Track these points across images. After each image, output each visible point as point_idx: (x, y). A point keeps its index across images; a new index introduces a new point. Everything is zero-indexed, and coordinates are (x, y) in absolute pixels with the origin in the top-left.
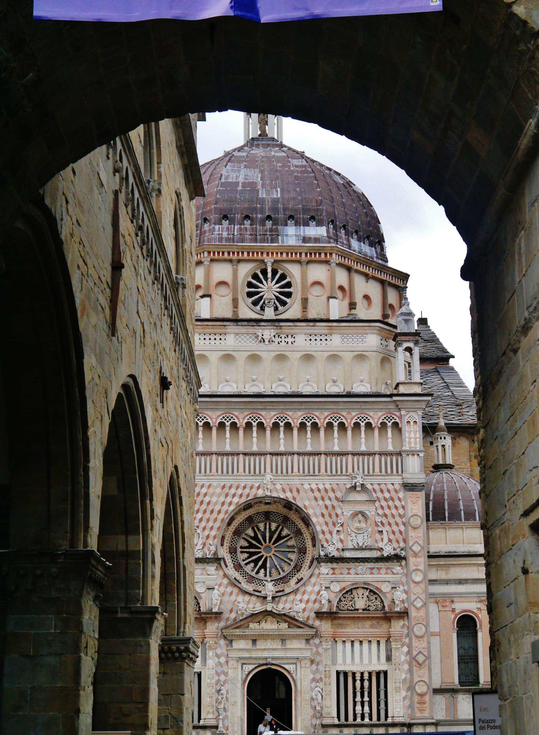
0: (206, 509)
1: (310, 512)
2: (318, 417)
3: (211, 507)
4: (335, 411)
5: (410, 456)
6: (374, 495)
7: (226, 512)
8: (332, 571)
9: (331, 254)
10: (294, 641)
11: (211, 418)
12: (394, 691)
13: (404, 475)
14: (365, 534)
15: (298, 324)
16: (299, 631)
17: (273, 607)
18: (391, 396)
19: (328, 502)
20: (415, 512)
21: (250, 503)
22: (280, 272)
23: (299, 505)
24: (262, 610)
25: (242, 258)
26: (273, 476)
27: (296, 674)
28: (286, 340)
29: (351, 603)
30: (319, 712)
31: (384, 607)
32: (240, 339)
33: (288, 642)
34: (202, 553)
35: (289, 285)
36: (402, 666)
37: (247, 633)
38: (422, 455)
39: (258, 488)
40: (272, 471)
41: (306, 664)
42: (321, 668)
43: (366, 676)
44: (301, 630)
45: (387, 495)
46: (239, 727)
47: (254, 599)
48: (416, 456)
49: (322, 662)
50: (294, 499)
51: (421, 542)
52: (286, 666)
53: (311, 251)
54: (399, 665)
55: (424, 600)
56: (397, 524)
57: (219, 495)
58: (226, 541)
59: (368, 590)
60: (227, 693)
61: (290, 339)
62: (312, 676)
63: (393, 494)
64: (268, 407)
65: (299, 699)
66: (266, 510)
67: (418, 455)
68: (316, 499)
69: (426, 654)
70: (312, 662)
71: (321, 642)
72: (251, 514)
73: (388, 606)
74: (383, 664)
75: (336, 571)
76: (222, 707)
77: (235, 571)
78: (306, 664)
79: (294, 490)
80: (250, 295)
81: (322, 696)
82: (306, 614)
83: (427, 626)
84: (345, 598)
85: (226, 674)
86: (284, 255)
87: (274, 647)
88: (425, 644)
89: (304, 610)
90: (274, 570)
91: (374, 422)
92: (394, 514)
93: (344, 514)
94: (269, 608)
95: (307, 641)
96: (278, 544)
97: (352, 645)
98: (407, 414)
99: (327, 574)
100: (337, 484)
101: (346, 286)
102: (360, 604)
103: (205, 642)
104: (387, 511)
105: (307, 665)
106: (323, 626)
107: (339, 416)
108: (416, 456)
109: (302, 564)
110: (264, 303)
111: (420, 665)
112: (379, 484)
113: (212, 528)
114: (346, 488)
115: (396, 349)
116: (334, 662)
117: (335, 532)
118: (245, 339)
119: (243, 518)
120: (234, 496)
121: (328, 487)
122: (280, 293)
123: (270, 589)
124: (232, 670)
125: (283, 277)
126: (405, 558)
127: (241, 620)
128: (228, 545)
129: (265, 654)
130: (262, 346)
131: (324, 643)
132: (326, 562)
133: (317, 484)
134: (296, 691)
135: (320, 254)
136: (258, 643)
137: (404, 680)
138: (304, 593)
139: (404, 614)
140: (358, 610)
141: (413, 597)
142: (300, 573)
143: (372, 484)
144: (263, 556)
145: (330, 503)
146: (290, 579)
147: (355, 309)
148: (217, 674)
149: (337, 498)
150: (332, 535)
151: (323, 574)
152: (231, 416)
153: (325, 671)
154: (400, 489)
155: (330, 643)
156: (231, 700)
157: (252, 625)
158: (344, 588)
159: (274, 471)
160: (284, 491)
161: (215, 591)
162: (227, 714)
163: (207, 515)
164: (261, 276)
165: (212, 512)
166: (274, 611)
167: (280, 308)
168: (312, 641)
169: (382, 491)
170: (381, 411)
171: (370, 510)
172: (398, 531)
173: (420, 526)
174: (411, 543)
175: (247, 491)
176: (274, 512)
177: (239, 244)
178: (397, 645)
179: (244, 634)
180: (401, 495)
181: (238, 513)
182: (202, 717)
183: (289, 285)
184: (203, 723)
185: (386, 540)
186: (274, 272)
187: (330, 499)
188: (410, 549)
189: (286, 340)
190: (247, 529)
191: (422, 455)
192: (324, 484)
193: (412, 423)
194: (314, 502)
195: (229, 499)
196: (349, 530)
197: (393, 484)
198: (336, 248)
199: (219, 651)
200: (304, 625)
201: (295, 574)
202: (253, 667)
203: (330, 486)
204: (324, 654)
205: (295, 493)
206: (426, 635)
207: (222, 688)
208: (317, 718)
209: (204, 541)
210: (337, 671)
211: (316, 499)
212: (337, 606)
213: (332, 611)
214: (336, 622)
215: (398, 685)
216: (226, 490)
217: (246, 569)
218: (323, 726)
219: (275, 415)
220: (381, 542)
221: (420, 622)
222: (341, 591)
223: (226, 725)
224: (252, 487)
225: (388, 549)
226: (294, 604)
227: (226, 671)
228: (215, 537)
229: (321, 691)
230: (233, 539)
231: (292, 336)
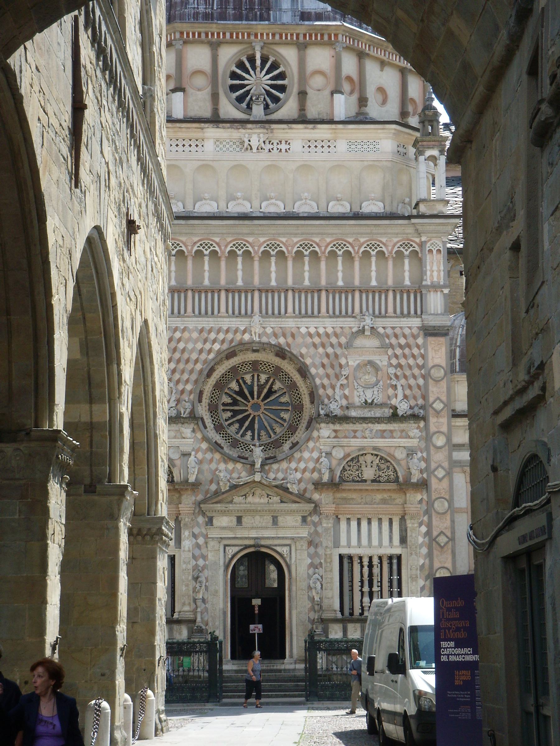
0: (180, 358)
1: (308, 361)
2: (318, 245)
3: (186, 356)
4: (340, 236)
5: (432, 293)
6: (387, 341)
7: (205, 362)
8: (333, 434)
9: (336, 36)
10: (289, 518)
11: (186, 246)
12: (409, 579)
13: (423, 316)
14: (375, 389)
15: (294, 126)
16: (294, 506)
17: (262, 477)
18: (409, 217)
19: (330, 350)
20: (437, 361)
21: (235, 350)
22: (272, 59)
23: (295, 352)
24: (249, 481)
25: (224, 40)
26: (262, 317)
27: (291, 557)
28: (279, 146)
29: (357, 472)
30: (318, 605)
31: (398, 477)
32: (221, 146)
33: (280, 519)
34: (175, 412)
35: (282, 76)
36: (420, 549)
37: (231, 508)
38: (446, 291)
39: (244, 332)
40: (261, 312)
41: (302, 546)
42: (321, 551)
43: (376, 561)
44: (297, 505)
45: (403, 341)
46: (222, 622)
47: (239, 466)
48: (439, 293)
49: (321, 542)
50: (288, 345)
51: (444, 399)
52: (278, 549)
53: (311, 32)
54: (416, 547)
55: (448, 470)
56: (415, 377)
57: (196, 341)
58: (204, 396)
59: (379, 457)
60: (207, 581)
61: (283, 147)
62: (309, 561)
63: (411, 340)
64: (256, 232)
65: (294, 588)
67: (442, 291)
68: (315, 345)
69: (449, 534)
70: (310, 543)
73: (402, 476)
74: (396, 547)
75: (339, 434)
76: (201, 597)
77: (216, 434)
78: (302, 546)
79: (289, 335)
80: (233, 88)
81: (322, 585)
82: (303, 486)
83: (450, 502)
84: (350, 466)
85: (205, 557)
86: (277, 37)
87: (264, 524)
88: (448, 523)
89: (300, 481)
90: (263, 433)
91: (388, 250)
92: (412, 364)
94: (257, 477)
95: (304, 519)
96: (269, 400)
97: (359, 524)
98: (429, 241)
99: (329, 437)
100: (341, 328)
101: (355, 76)
102: (369, 473)
103: (180, 519)
104: (403, 361)
105: (304, 548)
106: (323, 501)
107: (344, 243)
108: (439, 293)
109: (297, 425)
110: (251, 98)
111: (442, 547)
112: (393, 328)
113: (187, 381)
114: (353, 333)
115: (416, 159)
116: (337, 544)
118: (228, 146)
119: (226, 369)
120: (214, 341)
121: (330, 331)
122: (272, 86)
123: (258, 454)
124: (213, 554)
125: (275, 66)
126: (424, 419)
127: (223, 493)
128: (207, 401)
129: (253, 534)
130: (248, 155)
131: (324, 521)
132: (327, 423)
133: (316, 328)
134: (290, 579)
135: (322, 35)
136: (244, 520)
137: (422, 566)
138: (300, 460)
139: (423, 485)
140: (365, 481)
141: (433, 466)
142: (295, 436)
143: (384, 328)
144: (250, 414)
146: (283, 443)
147: (366, 106)
148: (194, 557)
149: (340, 345)
150: (334, 390)
151: (323, 438)
152: (211, 242)
153: (326, 555)
154: (419, 334)
155: (331, 521)
156: (211, 589)
157: (237, 499)
158: (349, 455)
159: (264, 311)
160: (275, 335)
161: (192, 457)
162: (207, 606)
163: (181, 366)
164: (248, 65)
165: (187, 361)
166: (264, 482)
167: (272, 106)
168: (309, 519)
169: (396, 336)
170: (396, 237)
171: (382, 360)
172: (416, 386)
173: (443, 379)
174: (431, 399)
175: (230, 336)
177: (219, 22)
178: (413, 524)
180: (420, 341)
181: (218, 362)
182: (176, 610)
183: (282, 76)
184: (177, 617)
185: (400, 397)
186: (264, 60)
187: (332, 345)
188: (431, 406)
189: (279, 146)
190: (230, 382)
191: (446, 291)
192: (325, 328)
193: (435, 252)
194: (312, 350)
195: (208, 346)
196: (356, 384)
197: (410, 328)
198: (343, 28)
200: (302, 497)
201: (289, 437)
202: (236, 549)
203: (332, 330)
205: (290, 340)
206: (449, 512)
207: (200, 574)
208: (315, 612)
209: (178, 397)
210: (340, 555)
211: (315, 345)
212: (340, 476)
213: (334, 482)
214: (339, 495)
215: (414, 572)
216: (205, 335)
217: (229, 431)
218: (322, 621)
219: (265, 242)
220: (395, 399)
221: (442, 496)
222: (344, 458)
223: (206, 619)
224: (236, 331)
225: (402, 407)
226: (288, 474)
227: (205, 554)
228: (191, 392)
229: (320, 578)
230: (213, 394)
231: (286, 141)
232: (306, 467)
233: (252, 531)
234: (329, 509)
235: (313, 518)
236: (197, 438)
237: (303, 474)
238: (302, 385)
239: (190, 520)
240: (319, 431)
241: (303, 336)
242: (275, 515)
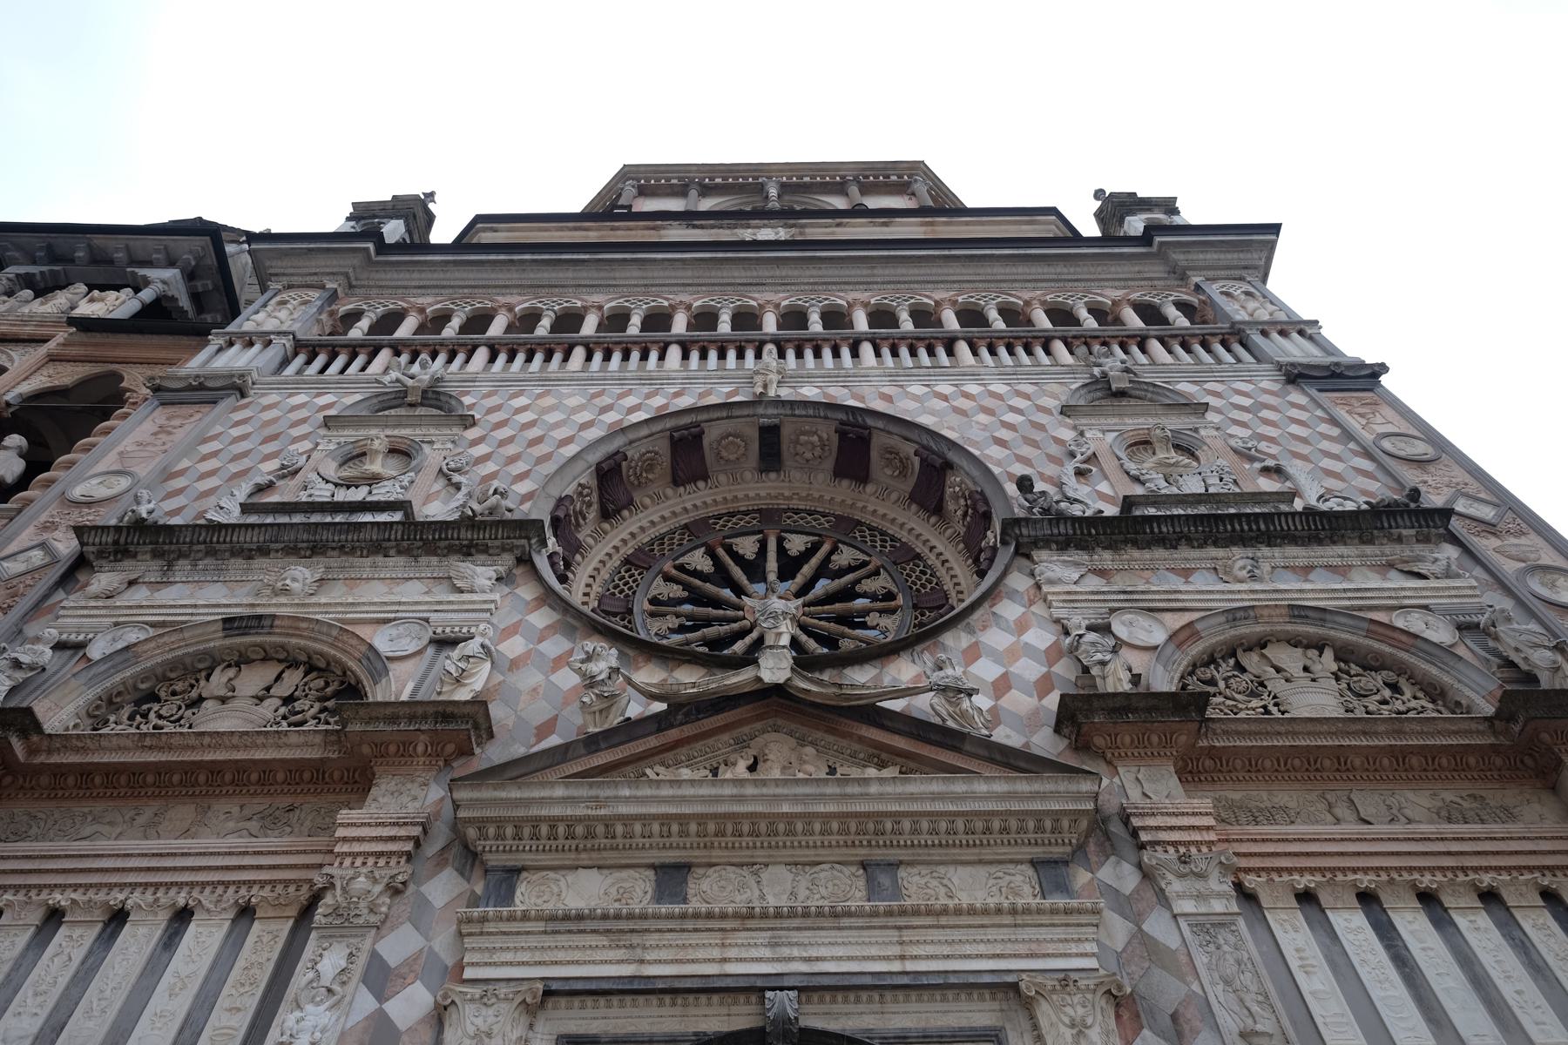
19: (1011, 418)
29: (1255, 703)
37: (623, 810)
53: (868, 173)
59: (1328, 654)
66: (763, 504)
68: (963, 413)
71: (1147, 875)
72: (702, 513)
93: (1088, 435)
108: (1295, 335)
117: (1070, 467)
121: (999, 388)
131: (1174, 886)
132: (1064, 545)
138: (973, 654)
145: (1020, 418)
155: (1219, 884)
176: (797, 512)
179: (603, 812)
194: (955, 419)
199: (398, 946)
204: (1201, 960)
232: (1005, 676)
233: (742, 937)
234: (1186, 821)
235: (1106, 873)
236: (523, 599)
237: (997, 698)
238: (934, 542)
239: (378, 888)
240: (1032, 575)
241: (915, 398)
242: (878, 854)
